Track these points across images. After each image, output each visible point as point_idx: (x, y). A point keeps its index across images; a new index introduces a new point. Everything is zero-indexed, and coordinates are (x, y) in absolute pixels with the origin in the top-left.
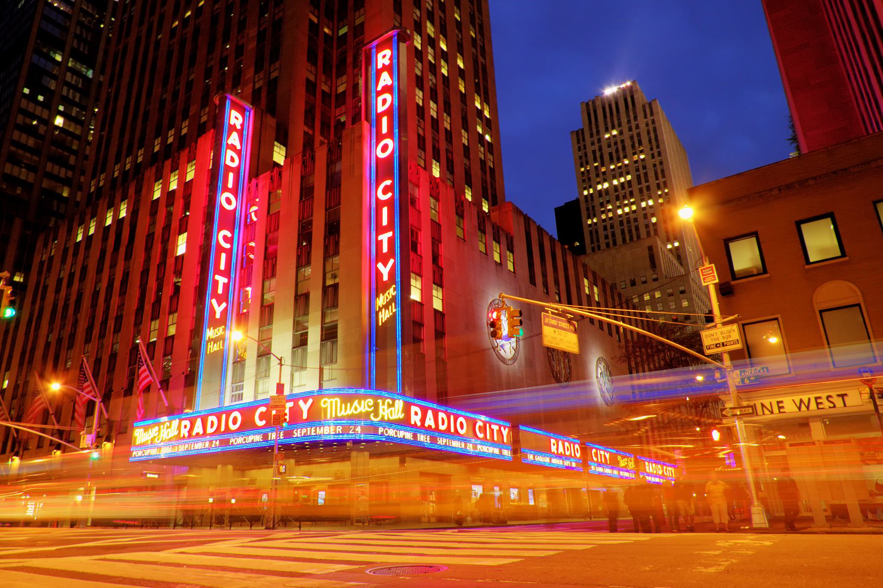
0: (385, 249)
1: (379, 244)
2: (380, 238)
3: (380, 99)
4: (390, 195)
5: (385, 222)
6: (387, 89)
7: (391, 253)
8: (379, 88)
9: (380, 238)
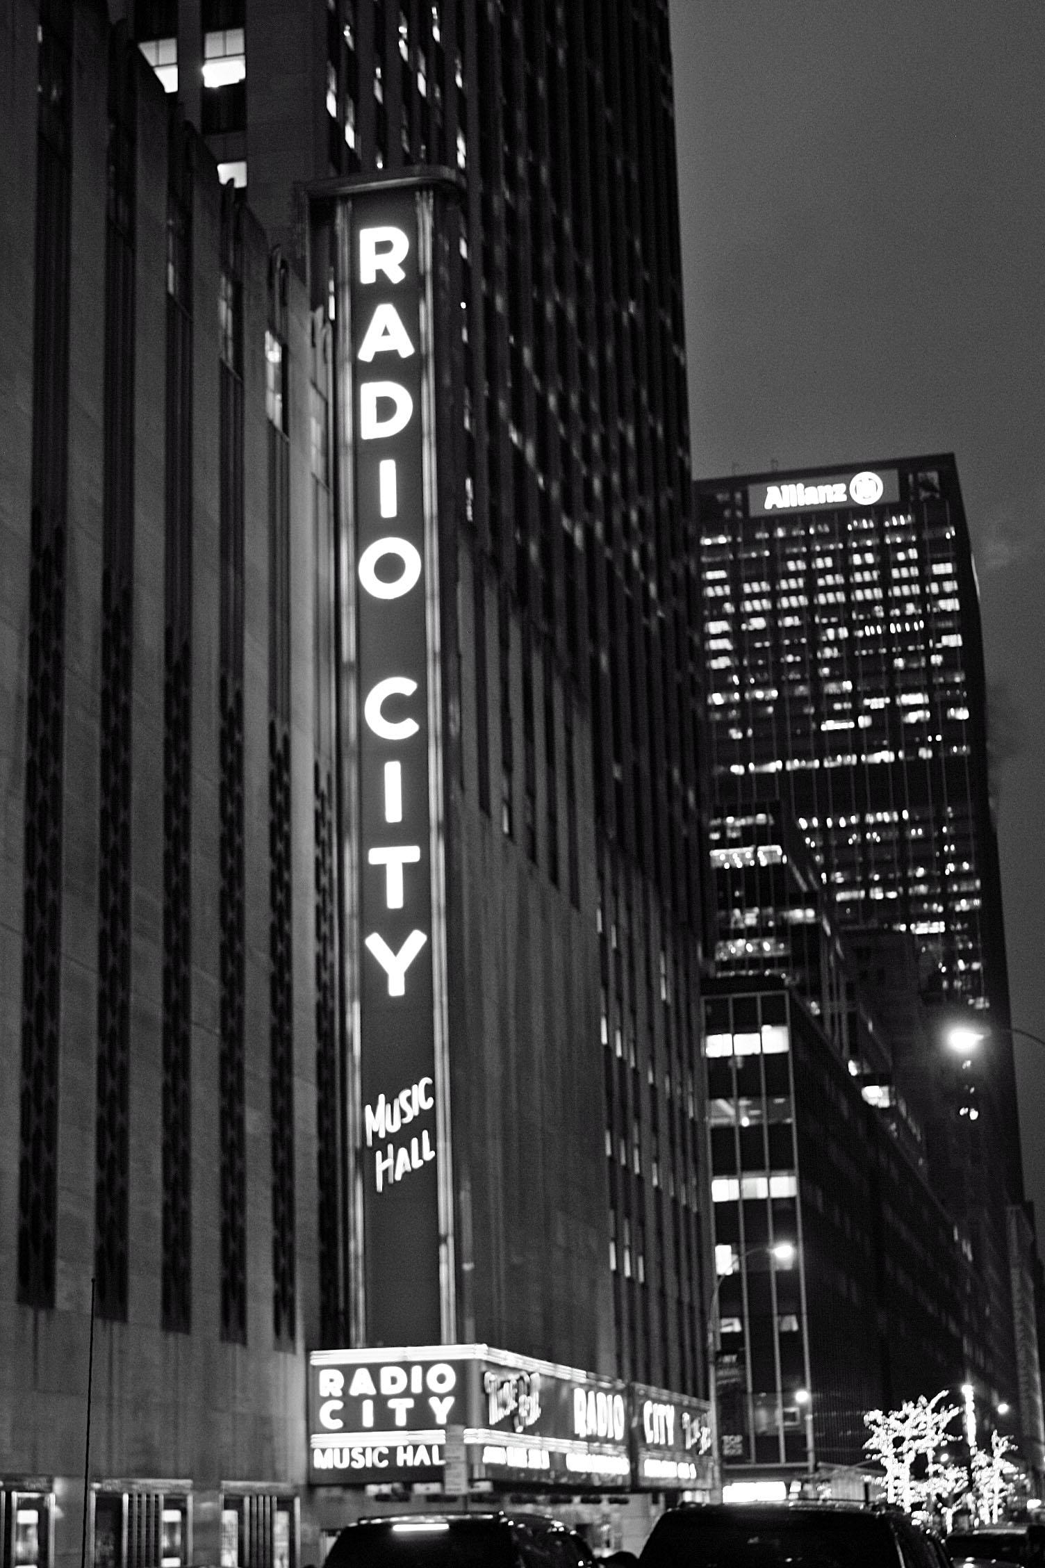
0: (395, 898)
1: (373, 878)
2: (376, 856)
3: (371, 391)
4: (407, 729)
5: (394, 812)
6: (387, 366)
7: (416, 913)
8: (366, 354)
9: (376, 856)
